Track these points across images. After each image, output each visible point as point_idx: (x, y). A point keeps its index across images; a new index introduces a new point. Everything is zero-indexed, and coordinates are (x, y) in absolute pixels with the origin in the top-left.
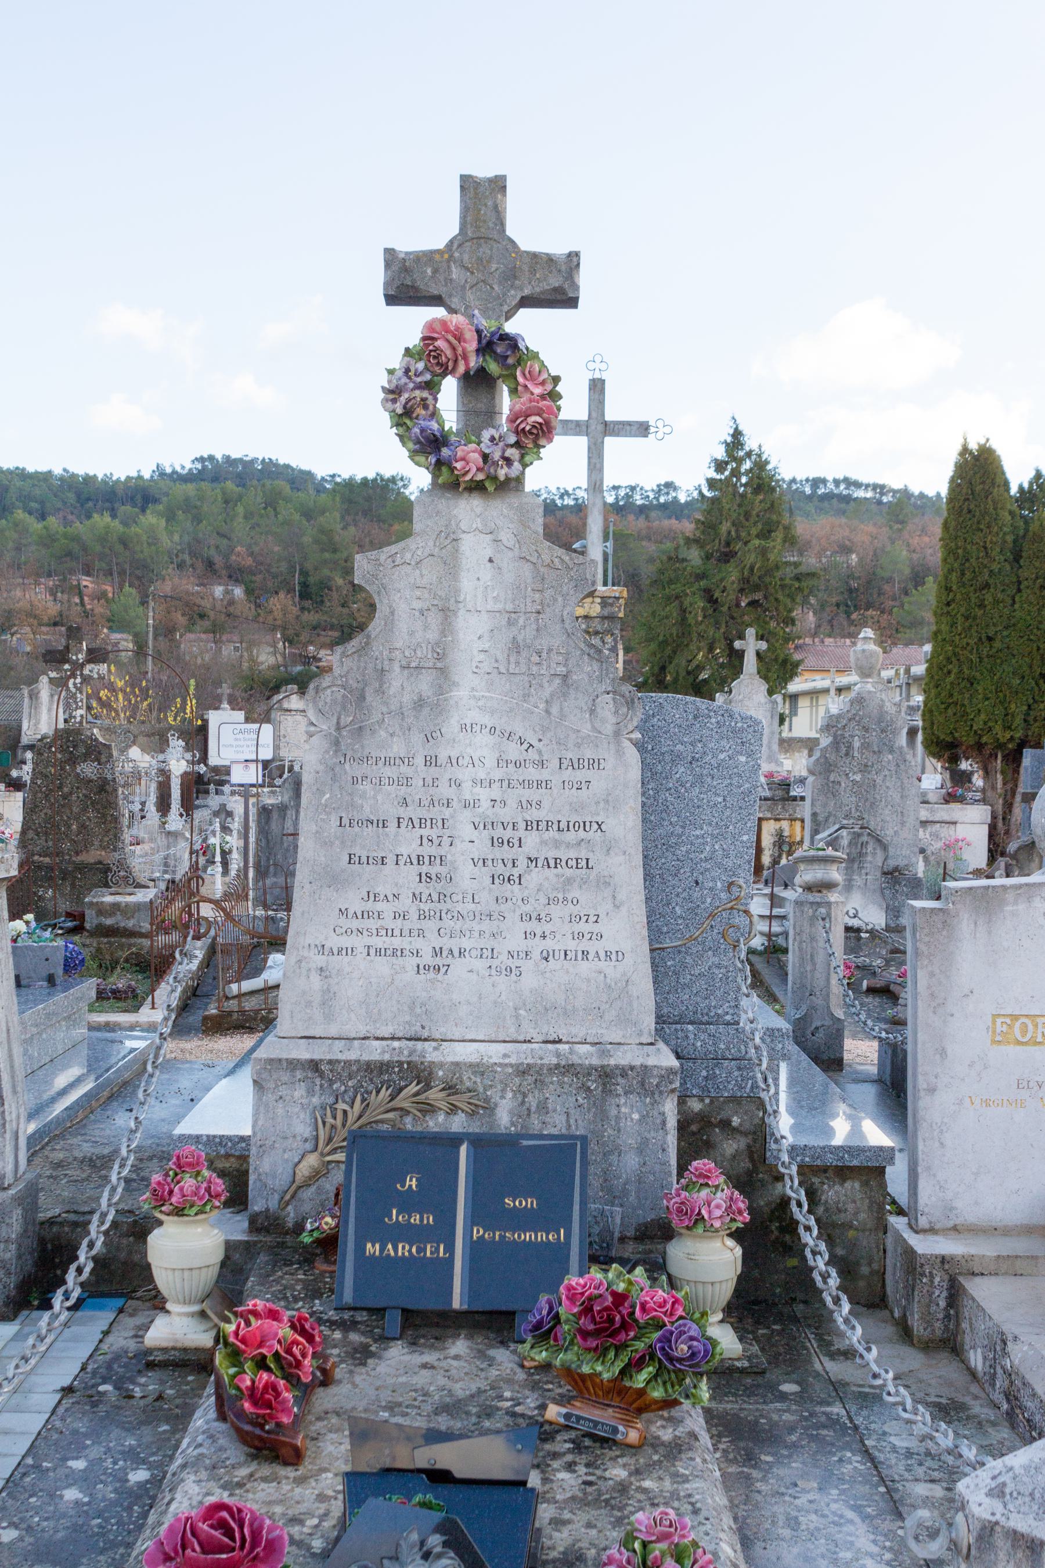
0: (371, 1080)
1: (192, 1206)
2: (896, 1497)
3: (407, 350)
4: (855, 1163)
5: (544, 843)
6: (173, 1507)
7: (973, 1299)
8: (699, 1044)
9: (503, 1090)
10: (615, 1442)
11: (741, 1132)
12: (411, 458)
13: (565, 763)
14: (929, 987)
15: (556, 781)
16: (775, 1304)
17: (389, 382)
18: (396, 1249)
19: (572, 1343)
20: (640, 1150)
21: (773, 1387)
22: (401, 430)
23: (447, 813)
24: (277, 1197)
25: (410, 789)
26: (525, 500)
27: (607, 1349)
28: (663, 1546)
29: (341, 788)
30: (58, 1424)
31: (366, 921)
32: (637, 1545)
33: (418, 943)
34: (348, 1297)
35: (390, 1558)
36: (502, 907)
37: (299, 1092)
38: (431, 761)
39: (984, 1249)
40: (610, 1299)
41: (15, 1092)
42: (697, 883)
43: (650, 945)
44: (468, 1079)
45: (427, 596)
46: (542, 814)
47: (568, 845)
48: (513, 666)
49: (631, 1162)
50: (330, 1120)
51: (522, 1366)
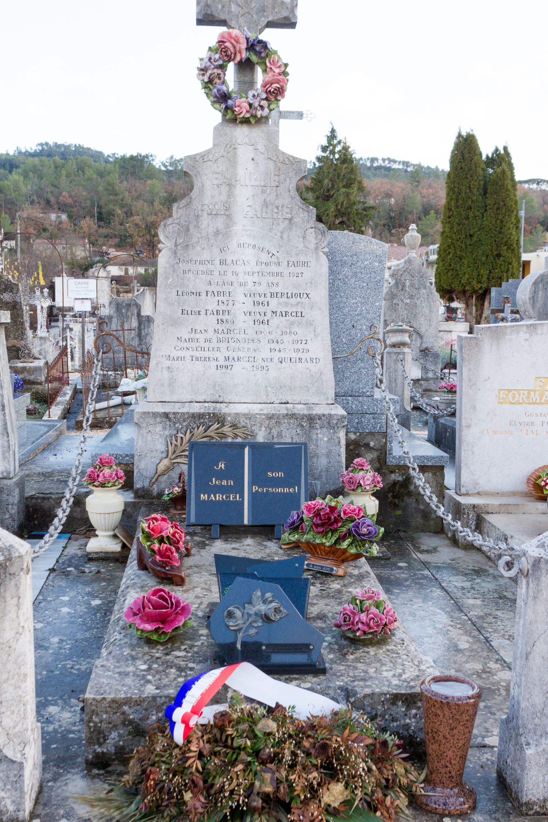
0: (195, 422)
1: (109, 483)
2: (459, 604)
3: (210, 48)
4: (430, 464)
5: (280, 304)
6: (127, 602)
7: (490, 523)
8: (354, 406)
9: (260, 427)
10: (331, 575)
11: (374, 449)
12: (212, 105)
13: (291, 263)
14: (468, 376)
15: (286, 272)
16: (390, 533)
17: (201, 65)
18: (215, 497)
19: (310, 530)
20: (328, 455)
21: (395, 564)
22: (207, 91)
23: (231, 289)
24: (148, 480)
25: (212, 277)
26: (270, 128)
27: (327, 533)
28: (370, 602)
29: (178, 276)
30: (51, 583)
31: (191, 343)
32: (358, 602)
33: (217, 354)
34: (193, 520)
35: (248, 603)
36: (259, 336)
37: (159, 428)
38: (223, 262)
39: (494, 502)
40: (328, 509)
41: (13, 432)
42: (353, 326)
43: (333, 355)
44: (243, 422)
45: (220, 177)
46: (279, 290)
47: (292, 305)
48: (264, 214)
49: (323, 462)
50: (174, 442)
51: (281, 548)
